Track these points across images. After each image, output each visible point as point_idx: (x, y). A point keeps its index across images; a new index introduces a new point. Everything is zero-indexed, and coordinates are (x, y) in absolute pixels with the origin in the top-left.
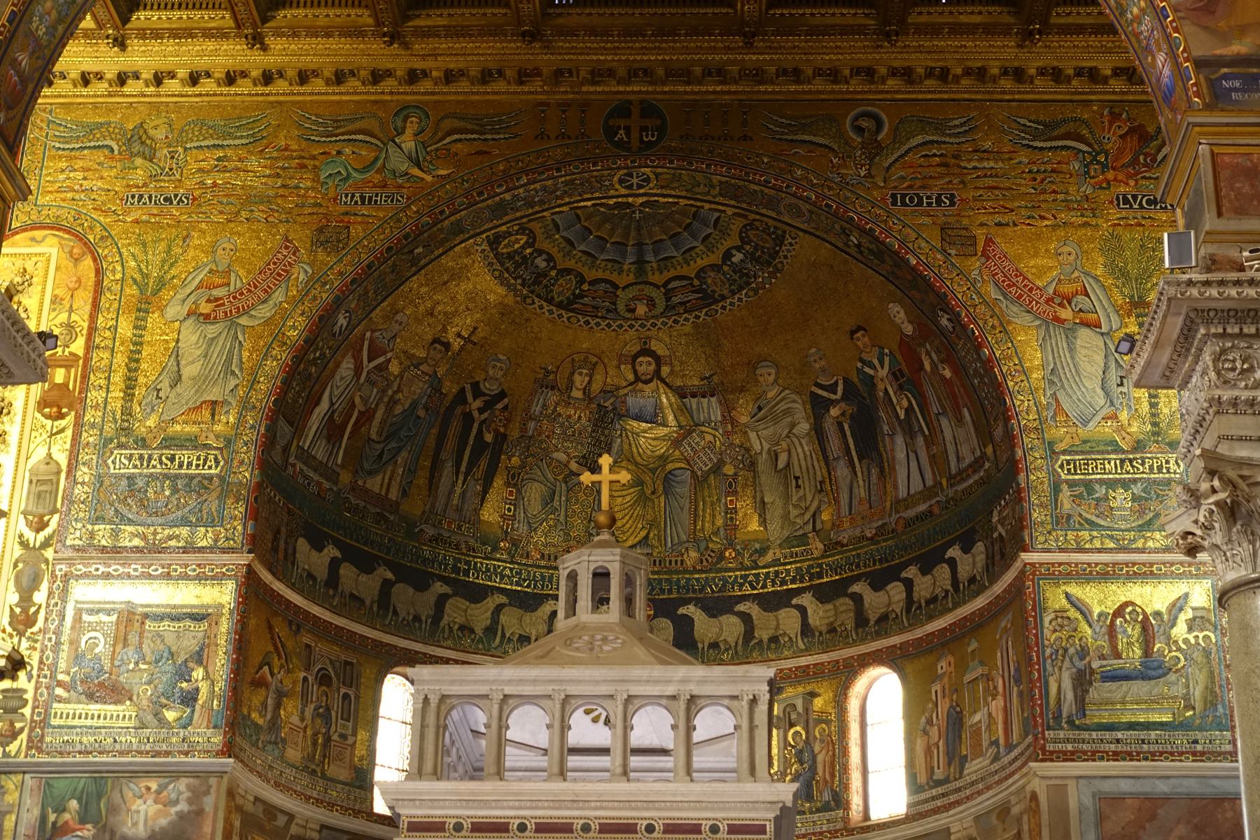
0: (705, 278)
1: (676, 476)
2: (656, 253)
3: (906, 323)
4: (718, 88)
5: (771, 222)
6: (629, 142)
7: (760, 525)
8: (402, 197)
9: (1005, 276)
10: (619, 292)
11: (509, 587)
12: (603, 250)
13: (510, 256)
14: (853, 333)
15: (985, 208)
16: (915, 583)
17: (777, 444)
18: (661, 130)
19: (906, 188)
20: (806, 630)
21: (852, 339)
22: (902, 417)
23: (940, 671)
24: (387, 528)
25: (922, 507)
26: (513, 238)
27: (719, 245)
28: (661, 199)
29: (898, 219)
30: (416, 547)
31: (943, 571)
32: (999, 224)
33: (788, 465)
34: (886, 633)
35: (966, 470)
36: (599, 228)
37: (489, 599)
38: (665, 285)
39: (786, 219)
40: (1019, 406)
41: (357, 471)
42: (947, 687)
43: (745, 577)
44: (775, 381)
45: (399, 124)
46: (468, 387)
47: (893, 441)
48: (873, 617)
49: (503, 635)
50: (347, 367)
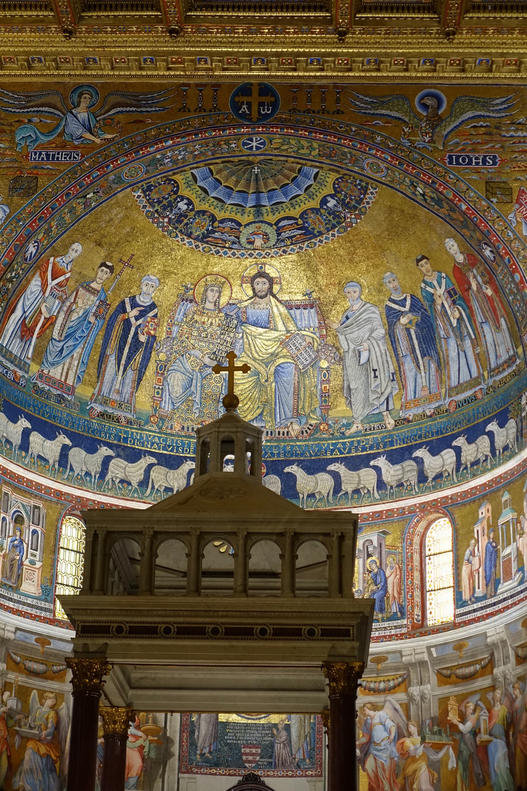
0: (306, 218)
1: (283, 368)
2: (270, 198)
3: (458, 253)
4: (318, 74)
6: (250, 114)
7: (347, 406)
8: (78, 155)
11: (158, 451)
12: (229, 196)
13: (159, 202)
14: (418, 261)
15: (519, 167)
16: (463, 450)
18: (275, 105)
19: (459, 151)
20: (381, 484)
21: (418, 265)
22: (455, 325)
23: (481, 516)
24: (66, 406)
25: (468, 393)
27: (318, 194)
28: (274, 158)
29: (454, 175)
30: (88, 421)
31: (484, 441)
34: (441, 487)
35: (502, 365)
36: (226, 181)
38: (277, 224)
41: (43, 363)
42: (486, 527)
45: (76, 99)
46: (127, 300)
47: (447, 343)
48: (431, 475)
49: (153, 487)
50: (35, 284)
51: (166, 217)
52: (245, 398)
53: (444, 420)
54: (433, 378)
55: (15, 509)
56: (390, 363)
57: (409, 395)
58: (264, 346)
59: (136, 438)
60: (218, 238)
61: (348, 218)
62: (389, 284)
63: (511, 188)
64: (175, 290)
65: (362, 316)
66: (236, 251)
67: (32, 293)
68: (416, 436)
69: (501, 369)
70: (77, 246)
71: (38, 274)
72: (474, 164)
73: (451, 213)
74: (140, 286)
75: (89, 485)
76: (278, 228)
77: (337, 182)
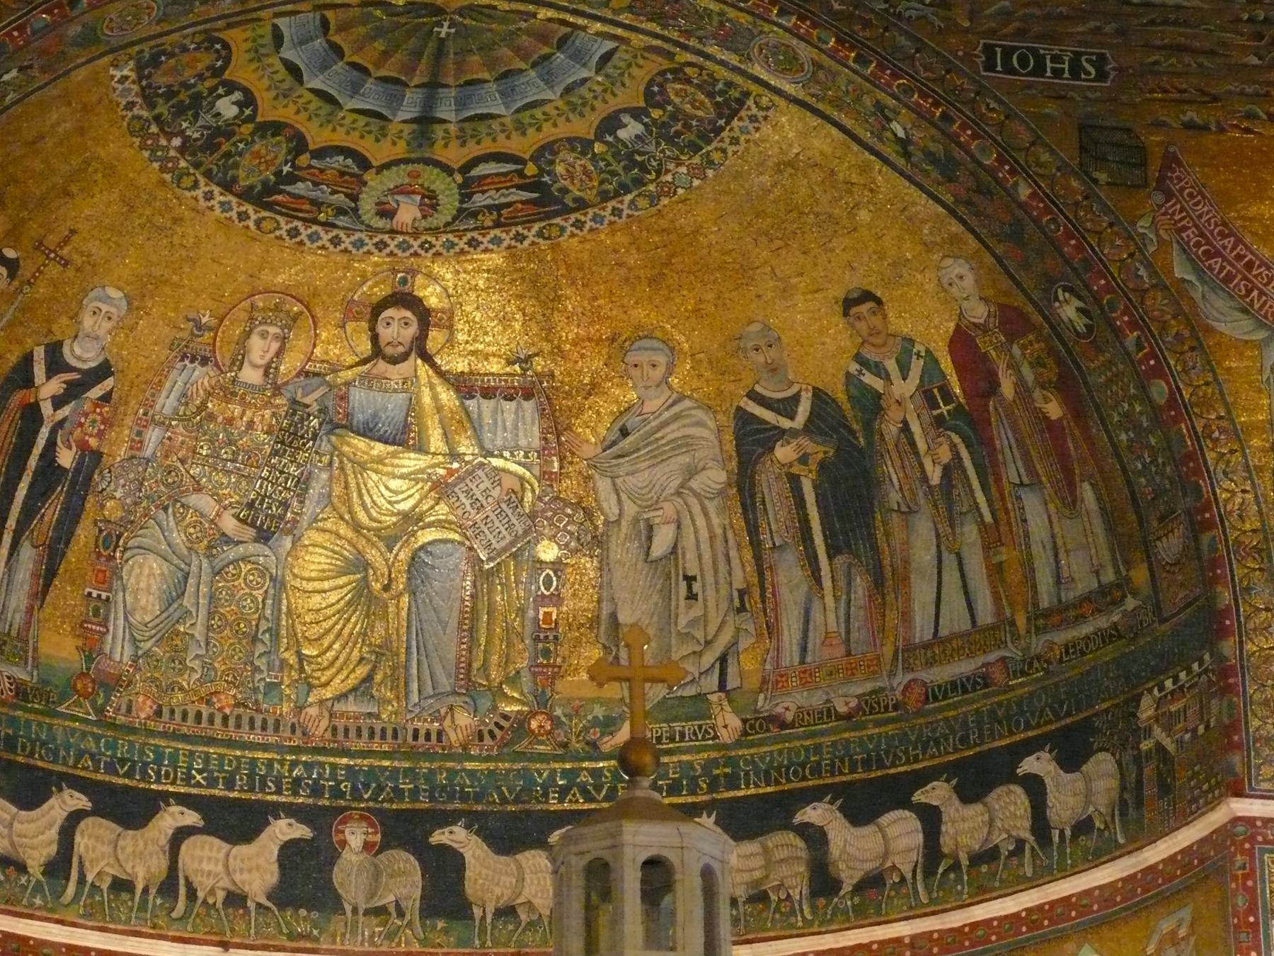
2: (461, 104)
5: (723, 73)
9: (1202, 235)
10: (367, 177)
11: (93, 776)
12: (355, 90)
13: (170, 94)
15: (1165, 91)
17: (655, 506)
26: (185, 58)
27: (597, 104)
29: (1000, 102)
32: (1189, 126)
33: (675, 547)
34: (879, 913)
37: (52, 801)
38: (465, 169)
39: (758, 70)
40: (1226, 501)
43: (570, 774)
44: (665, 381)
46: (39, 353)
47: (907, 527)
48: (849, 877)
49: (82, 880)
52: (328, 631)
53: (890, 729)
54: (858, 615)
56: (735, 562)
59: (38, 739)
60: (303, 197)
61: (667, 171)
63: (1144, 148)
64: (167, 329)
65: (668, 429)
66: (342, 235)
68: (803, 766)
69: (1072, 614)
72: (1049, 74)
73: (976, 198)
74: (76, 315)
77: (659, 79)
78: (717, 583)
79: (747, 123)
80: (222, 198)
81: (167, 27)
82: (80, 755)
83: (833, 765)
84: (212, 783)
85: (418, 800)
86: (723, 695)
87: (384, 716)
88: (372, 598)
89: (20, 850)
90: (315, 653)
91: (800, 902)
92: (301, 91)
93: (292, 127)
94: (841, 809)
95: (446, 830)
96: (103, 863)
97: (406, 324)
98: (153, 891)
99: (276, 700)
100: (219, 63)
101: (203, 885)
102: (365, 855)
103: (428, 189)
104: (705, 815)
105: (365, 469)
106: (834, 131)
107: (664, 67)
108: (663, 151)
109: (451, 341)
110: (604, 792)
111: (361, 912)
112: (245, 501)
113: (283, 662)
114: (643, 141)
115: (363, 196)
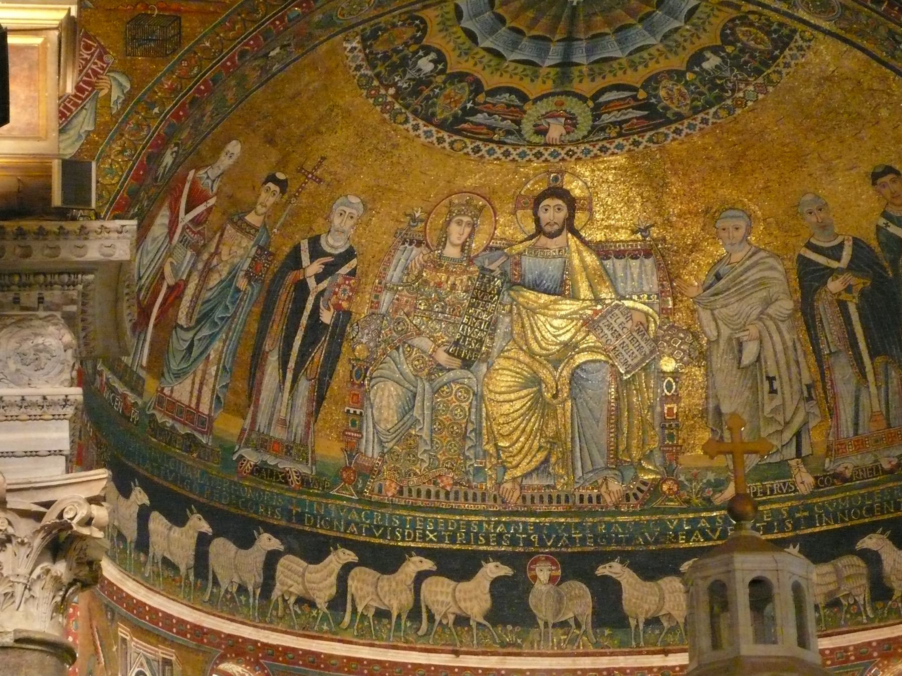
2: (590, 51)
5: (775, 17)
10: (526, 107)
13: (386, 57)
24: (199, 456)
26: (395, 32)
30: (235, 484)
33: (758, 359)
36: (516, 17)
37: (331, 557)
38: (595, 97)
39: (802, 14)
41: (163, 375)
43: (693, 522)
44: (745, 239)
46: (305, 245)
49: (354, 611)
51: (391, 86)
52: (516, 429)
55: (137, 670)
56: (803, 364)
57: (843, 428)
58: (551, 330)
60: (481, 124)
61: (740, 90)
62: (808, 216)
65: (749, 274)
66: (511, 149)
67: (154, 240)
68: (860, 508)
70: (234, 147)
71: (166, 204)
74: (329, 216)
75: (245, 610)
76: (596, 105)
77: (730, 25)
78: (790, 380)
79: (795, 52)
80: (425, 128)
81: (381, 11)
82: (348, 524)
83: (882, 507)
84: (440, 539)
85: (586, 545)
86: (800, 460)
87: (558, 487)
88: (546, 404)
89: (311, 592)
90: (507, 445)
91: (864, 605)
92: (476, 50)
93: (472, 75)
94: (890, 538)
95: (607, 565)
96: (368, 599)
97: (559, 209)
98: (404, 617)
99: (482, 479)
100: (419, 34)
101: (438, 611)
102: (551, 585)
103: (570, 113)
104: (791, 547)
105: (536, 313)
106: (859, 54)
107: (734, 16)
108: (735, 76)
109: (591, 219)
110: (718, 534)
111: (550, 625)
112: (453, 340)
113: (486, 452)
114: (721, 69)
115: (524, 121)
